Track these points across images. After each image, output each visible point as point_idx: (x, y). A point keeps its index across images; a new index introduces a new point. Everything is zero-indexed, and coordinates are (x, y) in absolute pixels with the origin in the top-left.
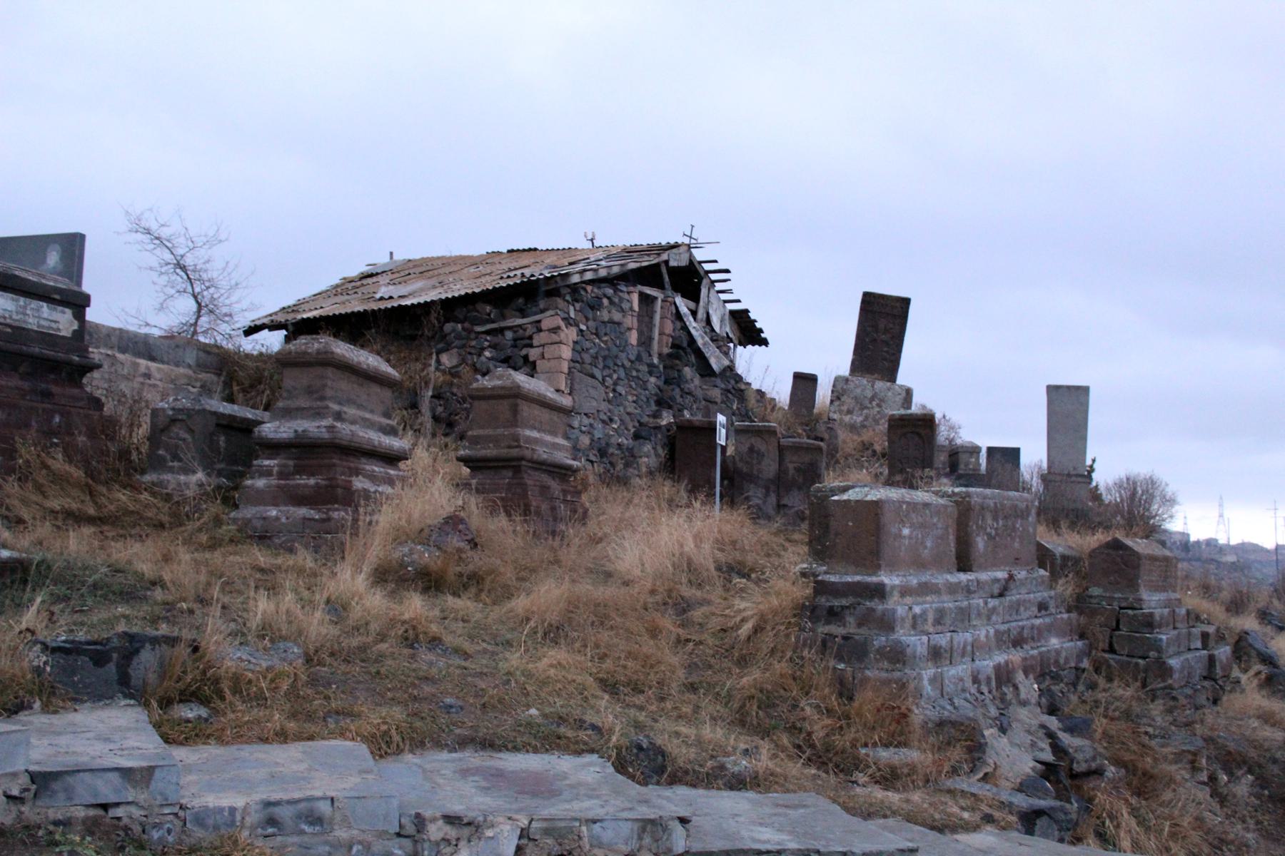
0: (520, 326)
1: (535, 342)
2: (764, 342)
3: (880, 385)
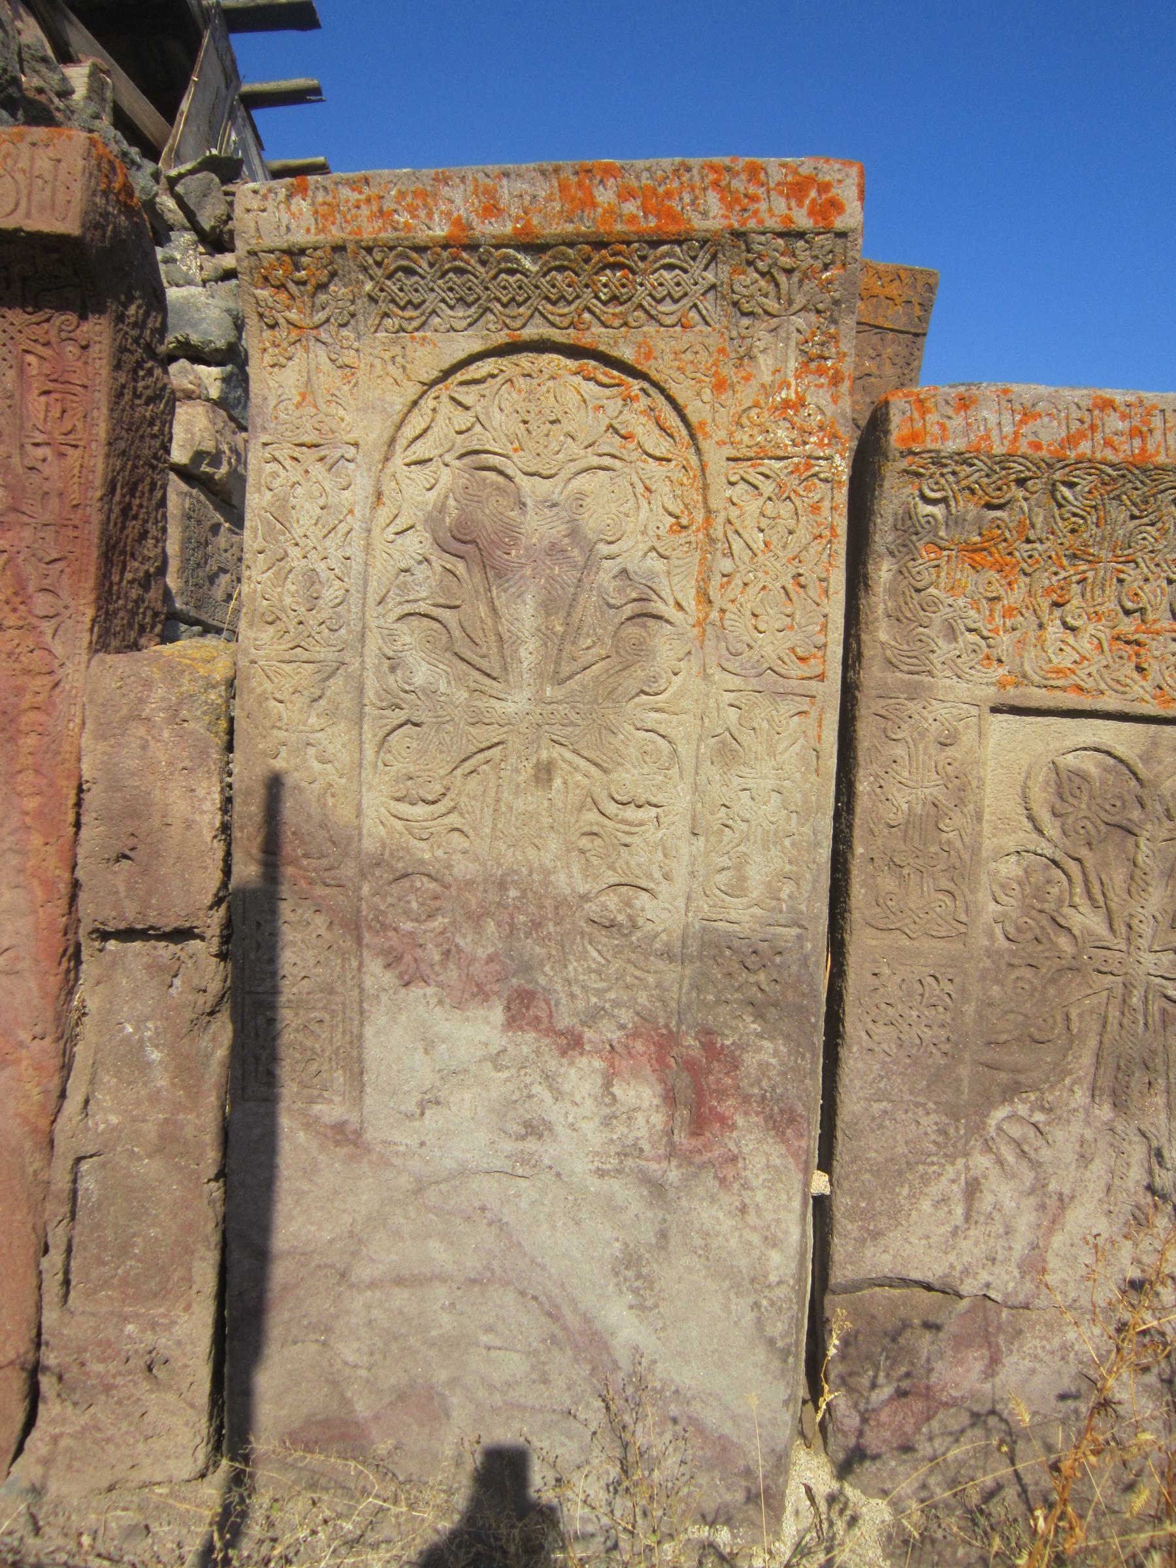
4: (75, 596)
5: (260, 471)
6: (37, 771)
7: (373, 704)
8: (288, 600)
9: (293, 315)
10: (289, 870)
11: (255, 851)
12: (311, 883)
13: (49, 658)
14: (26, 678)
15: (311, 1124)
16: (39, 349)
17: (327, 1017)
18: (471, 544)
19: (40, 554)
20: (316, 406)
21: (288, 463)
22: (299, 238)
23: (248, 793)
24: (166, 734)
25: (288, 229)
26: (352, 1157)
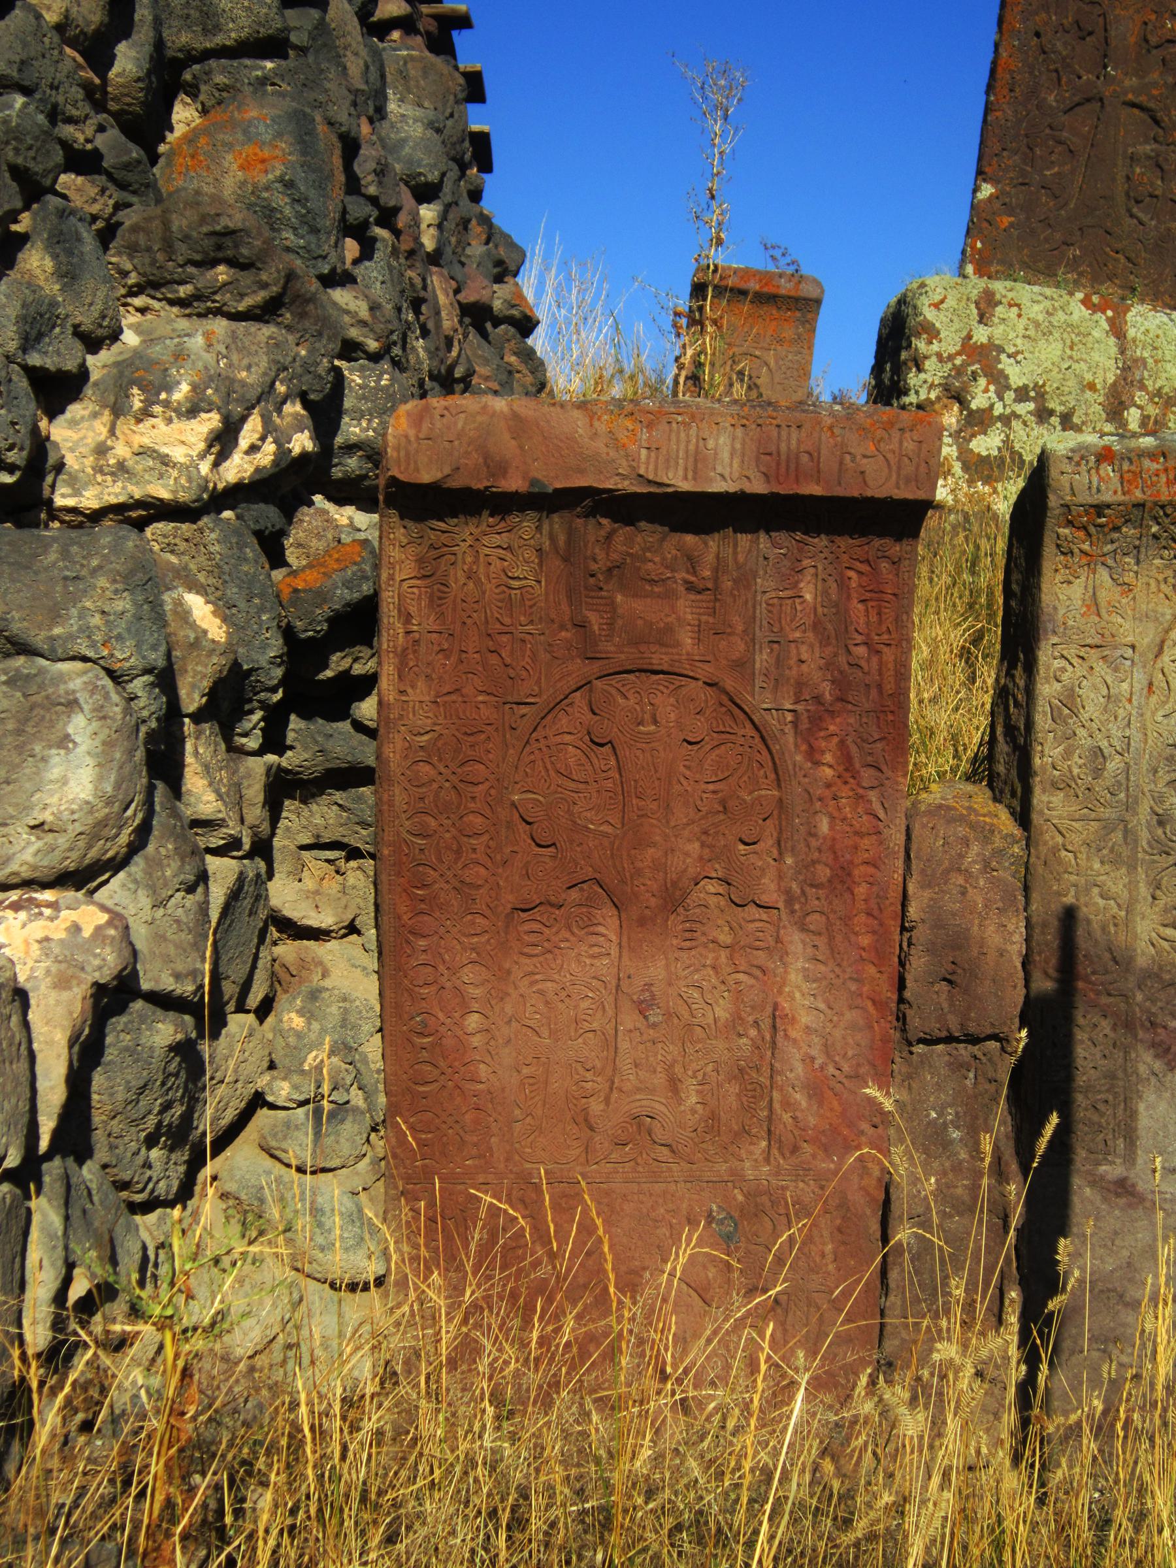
4: (894, 769)
5: (1048, 668)
6: (869, 914)
7: (1144, 851)
8: (1076, 771)
9: (1086, 547)
10: (1080, 985)
11: (1051, 971)
12: (1098, 993)
13: (875, 821)
14: (857, 839)
15: (1096, 1182)
16: (858, 565)
17: (1111, 1098)
19: (865, 736)
20: (1099, 615)
21: (1075, 661)
22: (1107, 497)
23: (1045, 925)
24: (982, 883)
25: (1099, 491)
26: (1130, 1206)
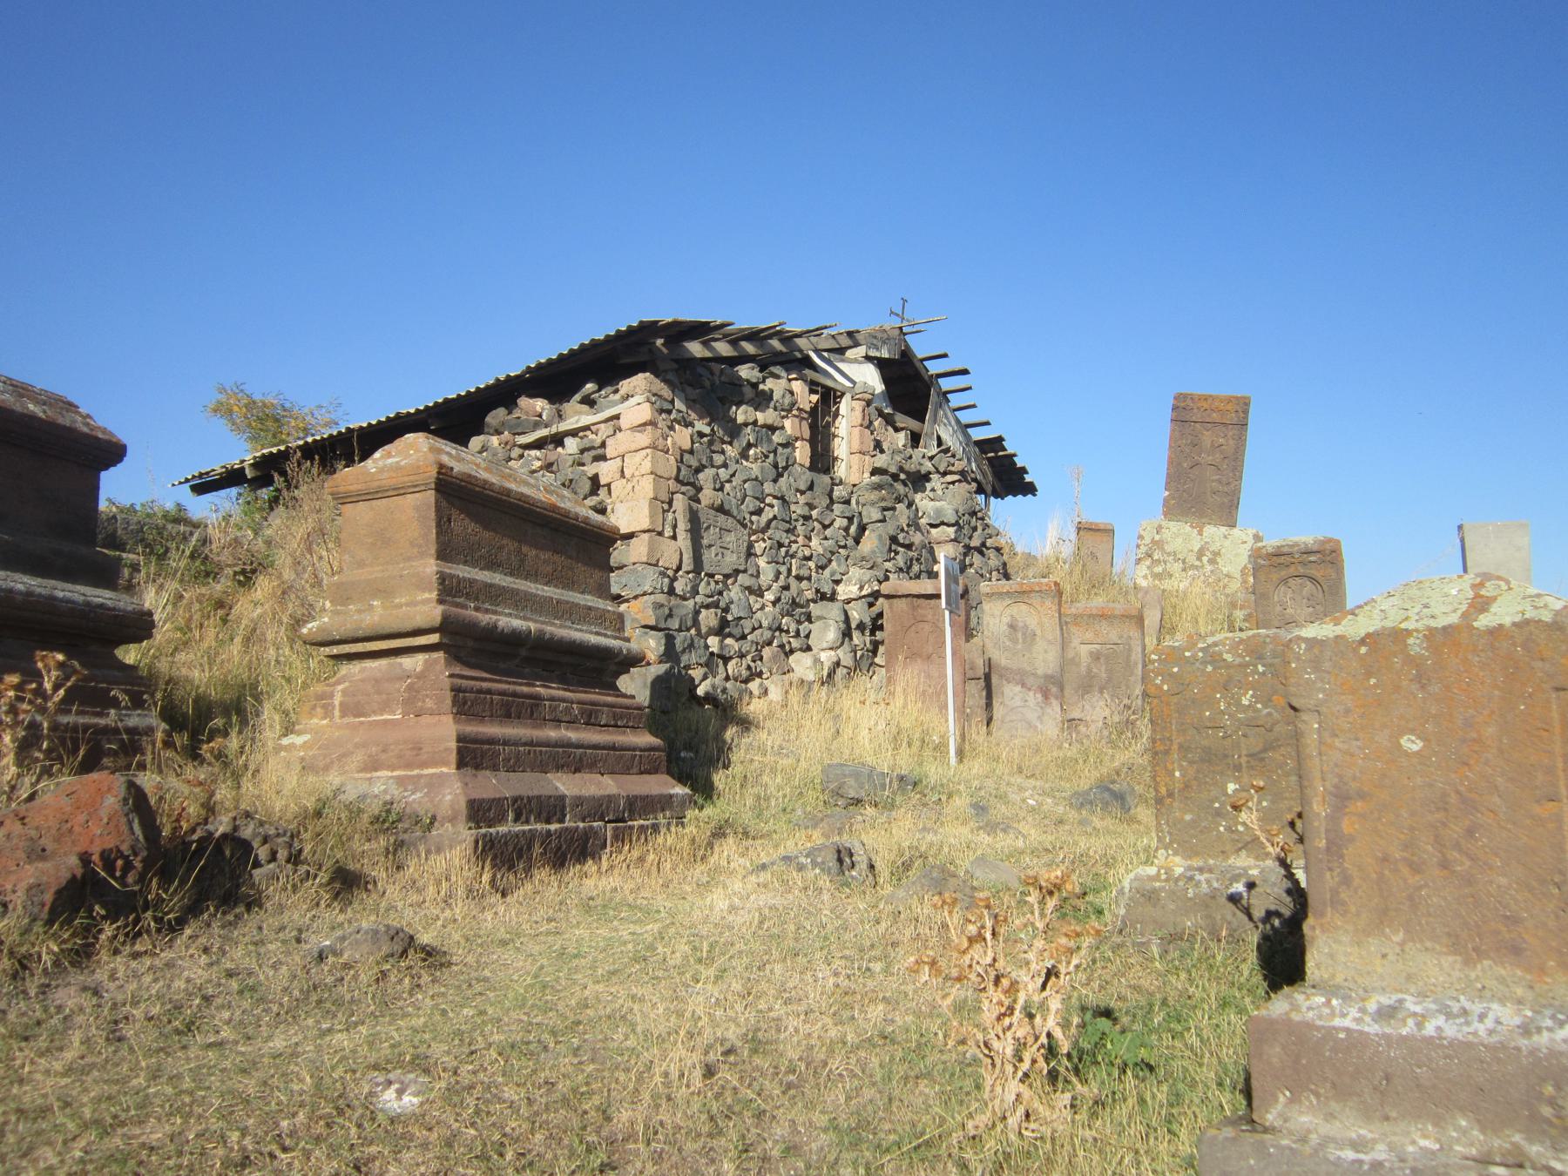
0: (587, 428)
1: (609, 452)
2: (1030, 489)
3: (1213, 532)
18: (1012, 627)
